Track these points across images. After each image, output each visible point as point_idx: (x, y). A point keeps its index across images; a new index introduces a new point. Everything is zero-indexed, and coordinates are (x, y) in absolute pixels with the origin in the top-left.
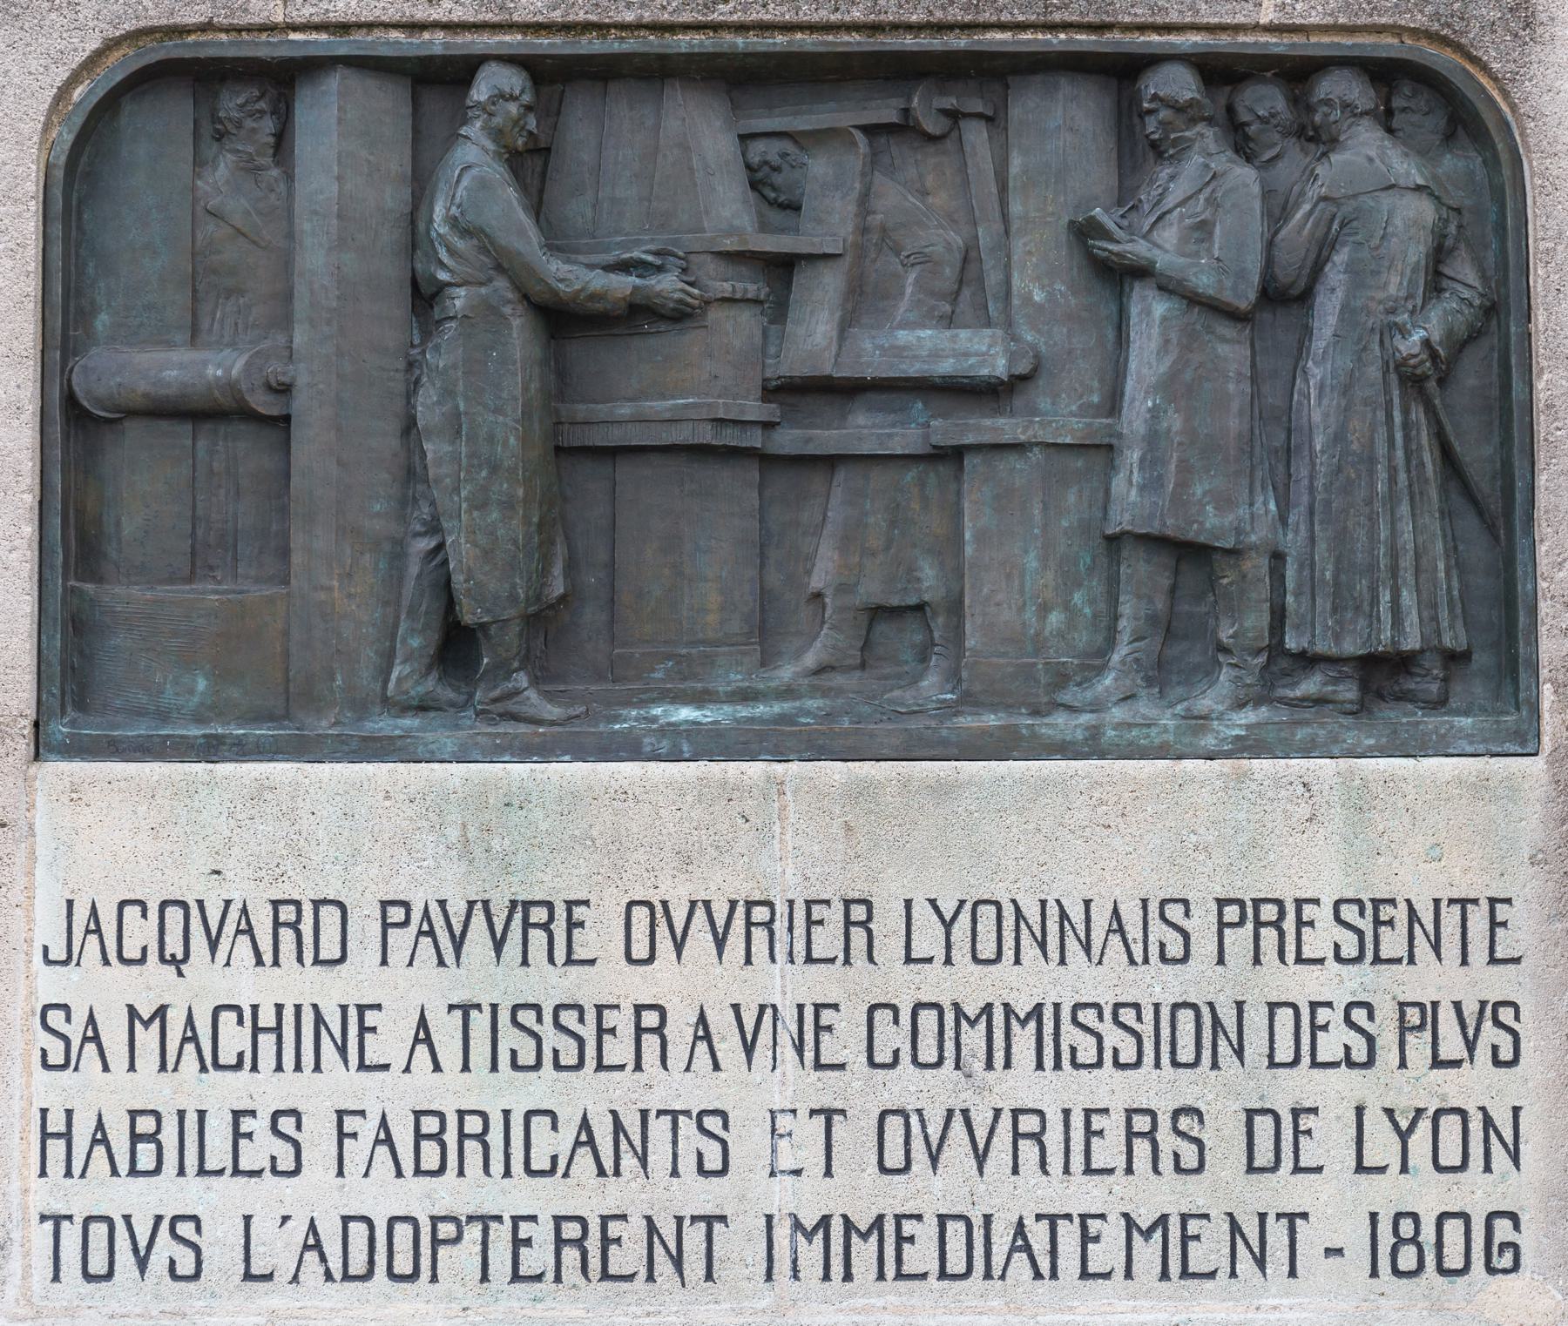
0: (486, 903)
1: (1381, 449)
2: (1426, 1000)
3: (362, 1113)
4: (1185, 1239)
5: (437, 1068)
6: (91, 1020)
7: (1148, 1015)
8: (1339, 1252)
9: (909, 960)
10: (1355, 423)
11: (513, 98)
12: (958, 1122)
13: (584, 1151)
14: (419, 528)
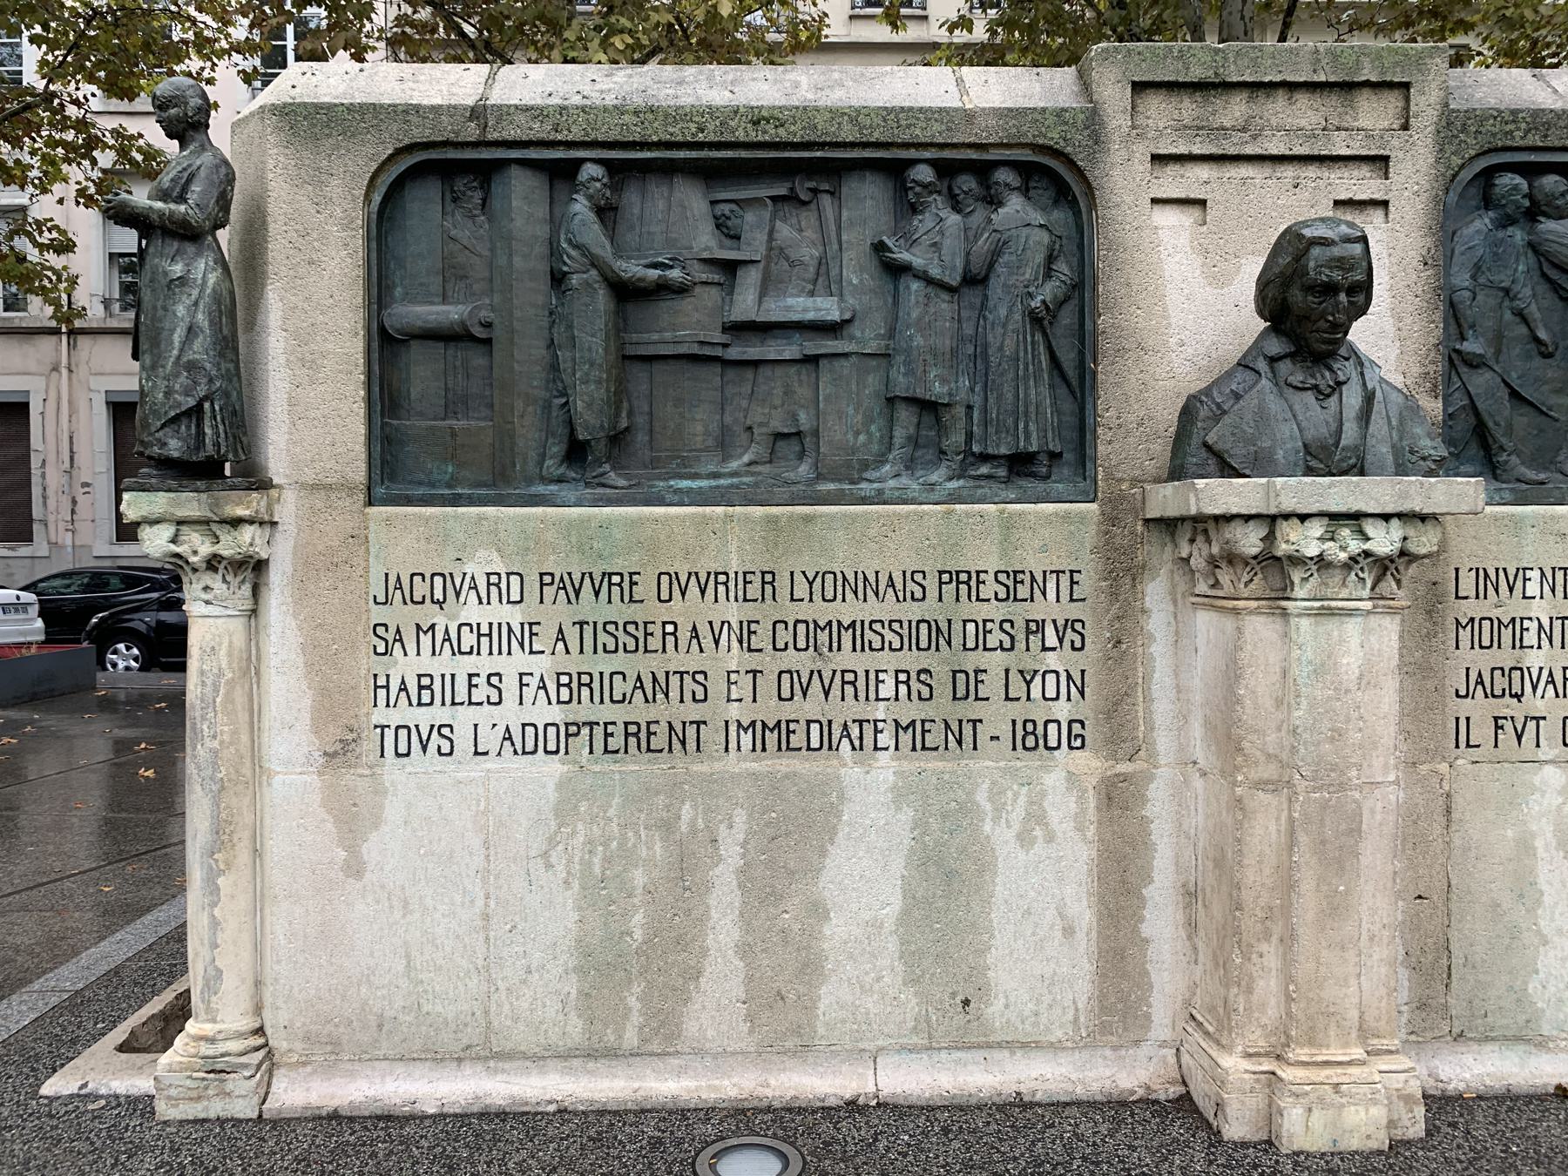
0: (591, 574)
1: (1022, 354)
2: (1039, 617)
3: (531, 674)
4: (924, 732)
5: (568, 652)
6: (398, 631)
7: (906, 625)
8: (998, 738)
9: (792, 599)
10: (1007, 342)
11: (598, 180)
12: (816, 675)
13: (639, 691)
14: (555, 393)
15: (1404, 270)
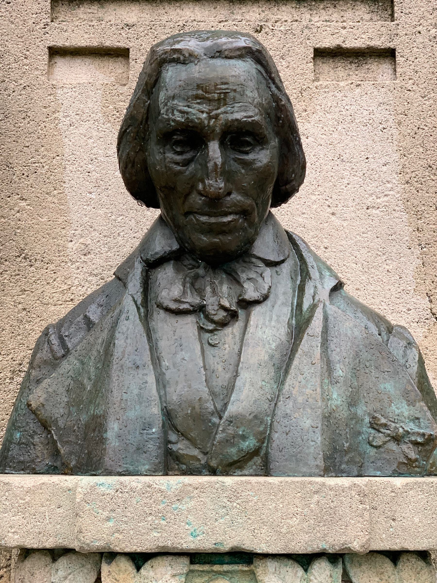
15: (422, 145)
